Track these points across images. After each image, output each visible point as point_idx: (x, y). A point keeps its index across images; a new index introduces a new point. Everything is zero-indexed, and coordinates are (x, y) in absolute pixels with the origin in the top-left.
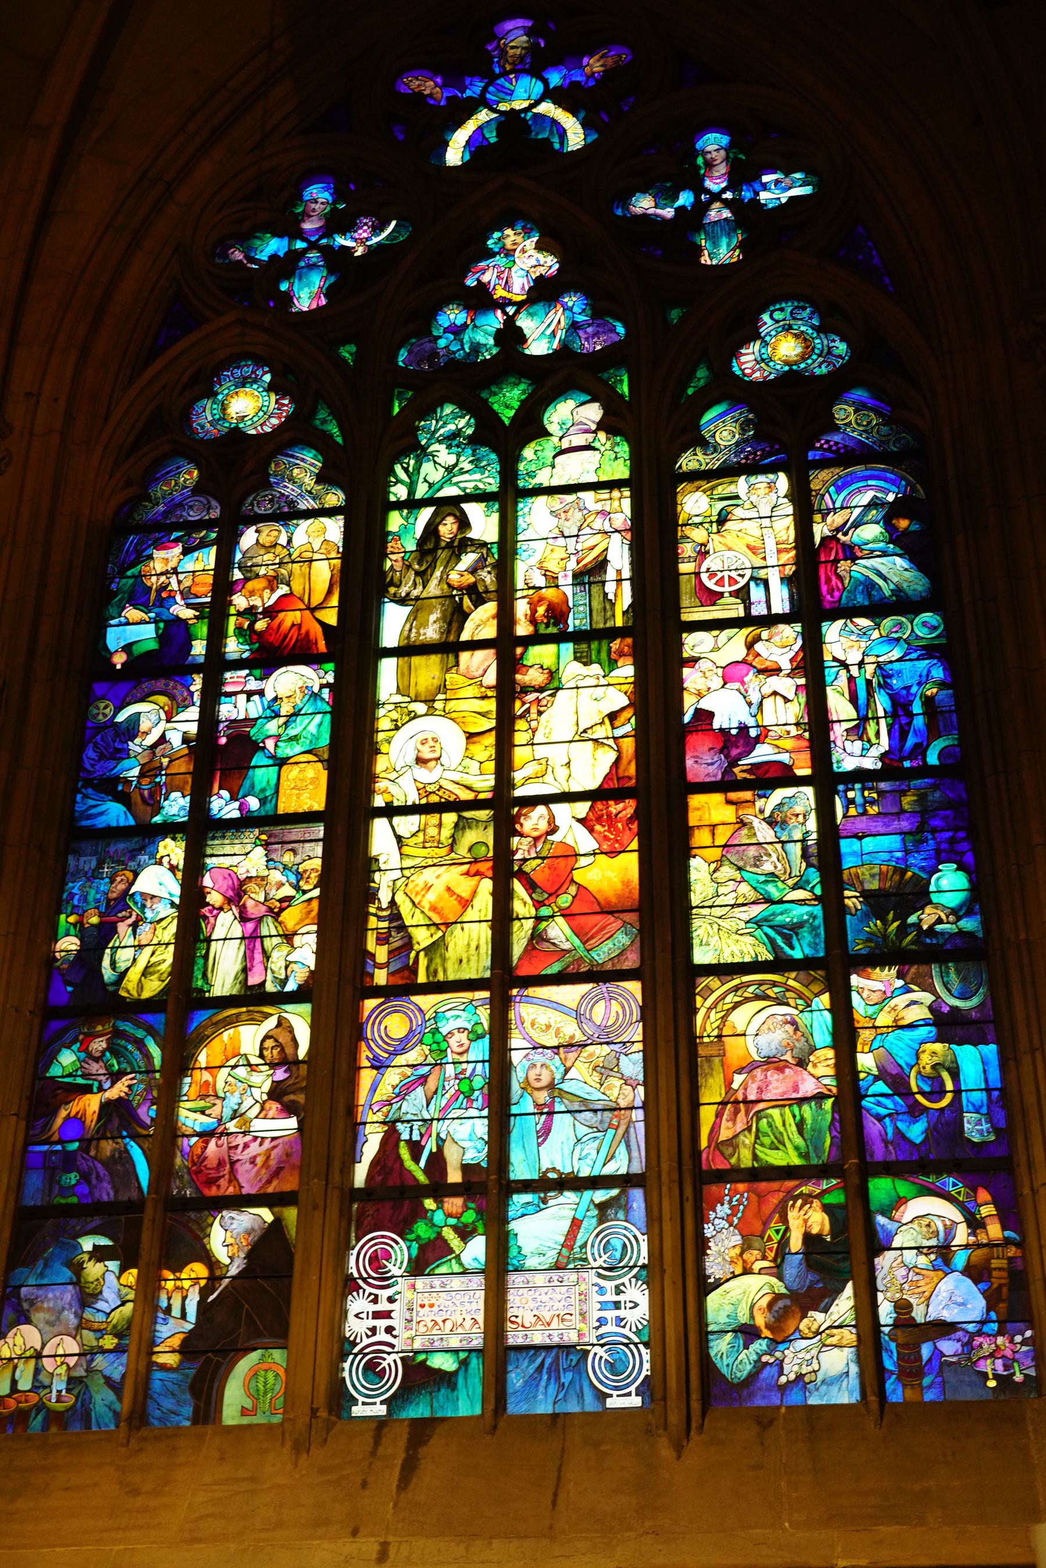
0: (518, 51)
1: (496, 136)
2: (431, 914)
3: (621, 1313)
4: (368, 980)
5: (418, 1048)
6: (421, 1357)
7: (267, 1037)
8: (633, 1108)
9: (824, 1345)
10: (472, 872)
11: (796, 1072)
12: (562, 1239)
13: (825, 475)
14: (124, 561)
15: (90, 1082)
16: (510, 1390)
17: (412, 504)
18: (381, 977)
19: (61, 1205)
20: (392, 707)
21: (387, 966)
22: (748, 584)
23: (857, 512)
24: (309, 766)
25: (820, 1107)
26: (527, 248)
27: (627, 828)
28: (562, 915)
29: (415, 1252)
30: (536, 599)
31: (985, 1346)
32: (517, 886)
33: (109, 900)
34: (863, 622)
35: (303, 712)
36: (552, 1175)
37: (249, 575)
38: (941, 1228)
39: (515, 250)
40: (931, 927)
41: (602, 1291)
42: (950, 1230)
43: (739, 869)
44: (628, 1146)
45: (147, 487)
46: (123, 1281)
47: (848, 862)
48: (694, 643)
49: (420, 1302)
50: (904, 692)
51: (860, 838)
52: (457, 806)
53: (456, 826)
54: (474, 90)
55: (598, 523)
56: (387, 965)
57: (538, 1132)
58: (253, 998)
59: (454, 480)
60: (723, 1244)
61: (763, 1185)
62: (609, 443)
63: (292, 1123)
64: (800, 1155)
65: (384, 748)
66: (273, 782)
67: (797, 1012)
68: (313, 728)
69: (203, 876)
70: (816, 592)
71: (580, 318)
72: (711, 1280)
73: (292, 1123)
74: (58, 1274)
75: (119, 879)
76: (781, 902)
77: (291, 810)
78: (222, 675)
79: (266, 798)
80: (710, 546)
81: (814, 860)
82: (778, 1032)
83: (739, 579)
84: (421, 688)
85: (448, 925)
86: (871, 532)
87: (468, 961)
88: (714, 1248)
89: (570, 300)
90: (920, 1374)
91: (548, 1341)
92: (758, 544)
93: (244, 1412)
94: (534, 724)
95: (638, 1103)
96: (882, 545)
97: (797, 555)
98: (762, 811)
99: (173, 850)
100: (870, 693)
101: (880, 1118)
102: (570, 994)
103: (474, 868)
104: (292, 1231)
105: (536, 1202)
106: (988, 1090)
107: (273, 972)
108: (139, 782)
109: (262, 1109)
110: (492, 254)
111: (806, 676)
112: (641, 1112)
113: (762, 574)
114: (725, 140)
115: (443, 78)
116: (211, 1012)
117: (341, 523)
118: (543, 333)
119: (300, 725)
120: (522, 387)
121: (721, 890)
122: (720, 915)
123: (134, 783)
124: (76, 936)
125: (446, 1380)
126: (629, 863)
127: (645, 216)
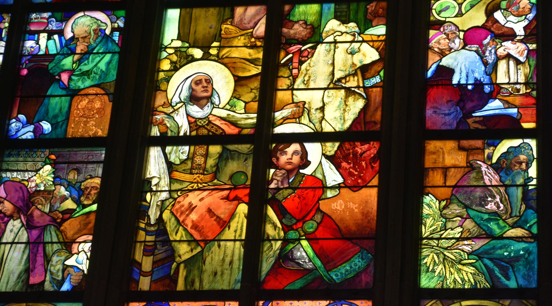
2: (193, 232)
4: (134, 285)
10: (232, 196)
18: (145, 284)
20: (171, 51)
21: (151, 275)
27: (370, 167)
32: (271, 213)
35: (95, 51)
43: (466, 207)
52: (222, 139)
56: (151, 273)
65: (163, 88)
66: (65, 110)
68: (102, 66)
76: (501, 238)
77: (78, 135)
78: (28, 15)
79: (58, 123)
81: (533, 203)
84: (199, 35)
85: (207, 242)
87: (222, 274)
94: (295, 71)
98: (490, 157)
103: (233, 194)
111: (536, 42)
119: (92, 62)
121: (449, 225)
122: (446, 246)
126: (370, 195)
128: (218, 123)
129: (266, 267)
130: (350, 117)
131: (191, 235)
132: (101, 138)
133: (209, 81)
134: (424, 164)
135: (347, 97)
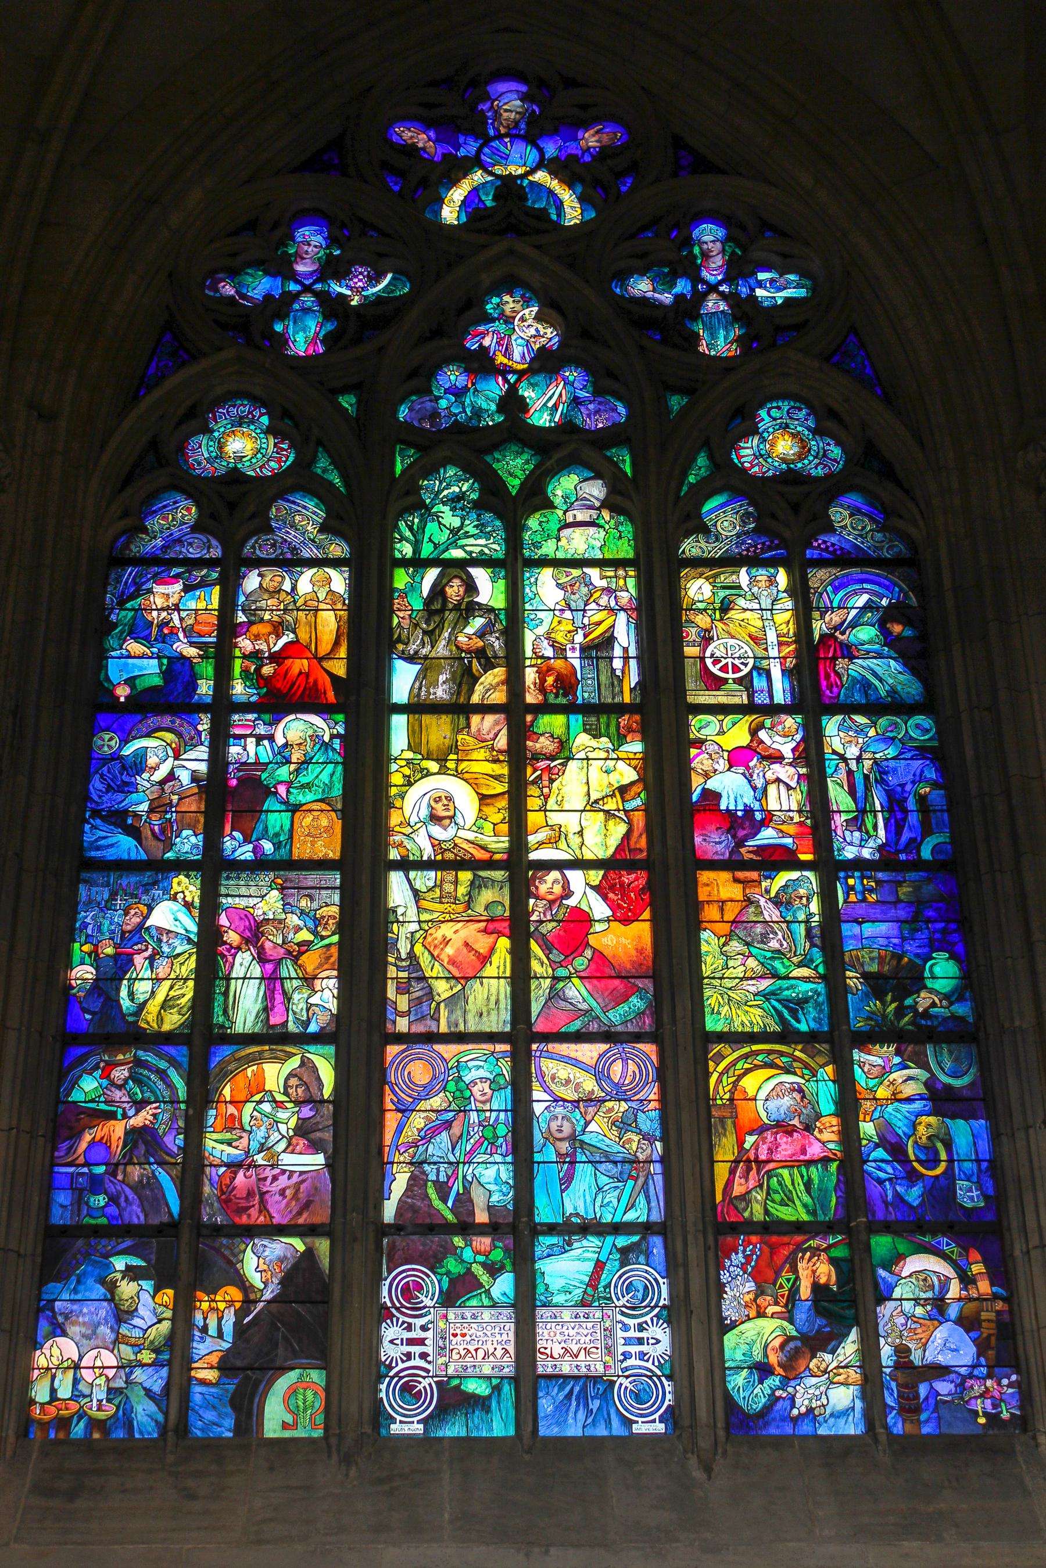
0: (513, 115)
1: (493, 200)
2: (450, 967)
3: (644, 1348)
5: (442, 1094)
6: (456, 1382)
9: (832, 1383)
11: (803, 1137)
12: (587, 1279)
14: (123, 592)
16: (541, 1414)
17: (418, 563)
19: (90, 1226)
22: (750, 673)
23: (853, 612)
25: (826, 1168)
28: (581, 978)
29: (445, 1286)
32: (534, 946)
33: (123, 933)
34: (861, 719)
38: (936, 1282)
40: (926, 1010)
41: (626, 1328)
43: (747, 944)
45: (144, 519)
46: (158, 1299)
47: (849, 946)
50: (899, 789)
51: (860, 923)
53: (472, 883)
54: (469, 148)
56: (408, 1013)
58: (274, 1038)
60: (738, 1288)
61: (774, 1238)
62: (613, 522)
63: (320, 1159)
64: (808, 1212)
65: (398, 804)
66: (287, 827)
68: (325, 777)
70: (816, 684)
71: (582, 394)
73: (320, 1159)
74: (91, 1290)
75: (133, 912)
76: (787, 978)
77: (306, 856)
80: (714, 633)
83: (742, 667)
84: (433, 746)
86: (866, 634)
88: (729, 1293)
89: (571, 374)
90: (917, 1410)
92: (760, 634)
93: (285, 1426)
96: (877, 647)
98: (768, 891)
99: (187, 886)
100: (867, 788)
101: (880, 1182)
102: (589, 1052)
104: (325, 1262)
106: (978, 1161)
107: (294, 1013)
109: (289, 1144)
110: (490, 319)
111: (807, 766)
112: (658, 1166)
114: (721, 233)
116: (235, 1047)
117: (346, 575)
118: (545, 405)
120: (525, 456)
121: (731, 963)
125: (480, 1403)
126: (641, 930)
128: (465, 846)
129: (535, 1008)
130: (614, 842)
132: (332, 861)
133: (450, 799)
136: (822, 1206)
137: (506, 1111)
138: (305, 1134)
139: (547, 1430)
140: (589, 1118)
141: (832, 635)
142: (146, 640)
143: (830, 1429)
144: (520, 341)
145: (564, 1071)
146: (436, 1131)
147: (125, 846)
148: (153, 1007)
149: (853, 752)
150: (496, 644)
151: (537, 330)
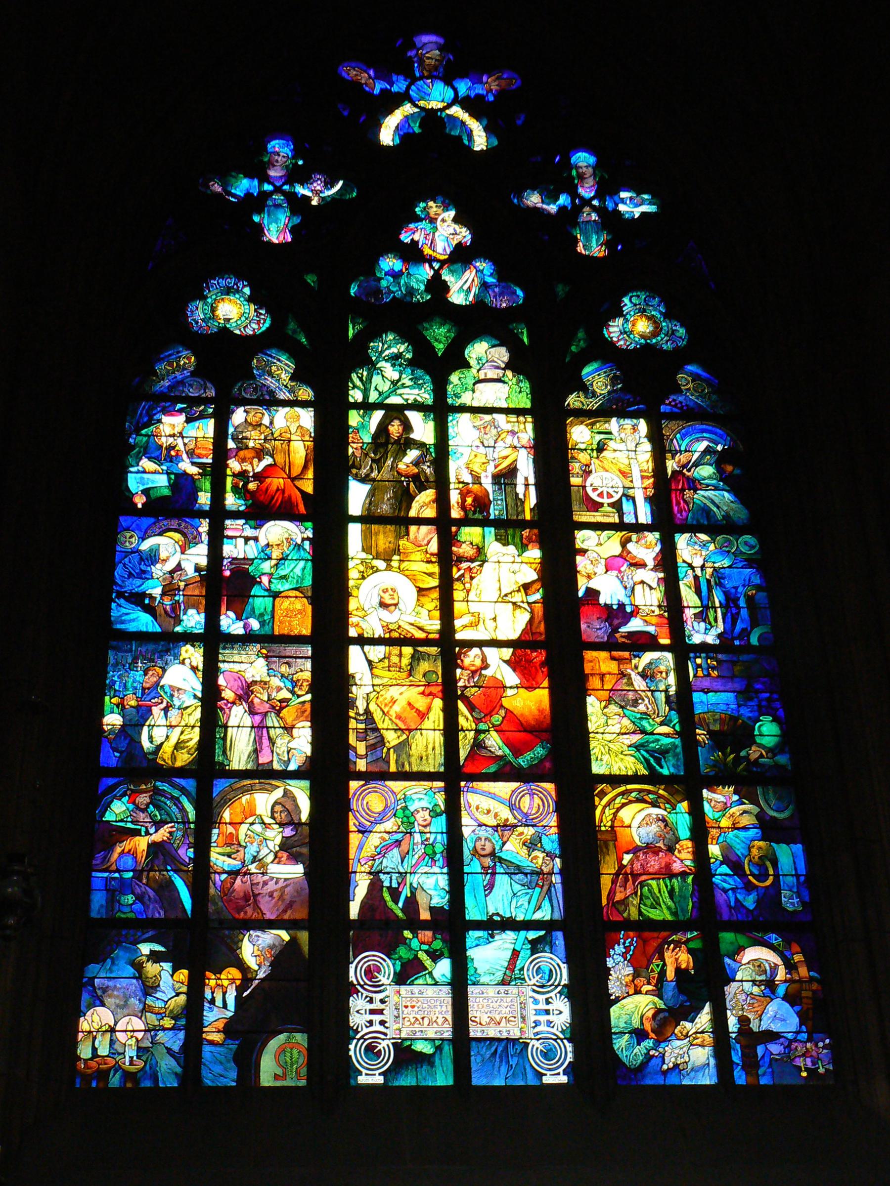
1: (420, 127)
5: (393, 819)
6: (409, 1043)
7: (276, 803)
8: (553, 873)
9: (692, 1045)
10: (427, 692)
12: (506, 964)
13: (673, 425)
14: (138, 422)
15: (139, 827)
17: (366, 407)
18: (361, 765)
19: (121, 919)
20: (359, 561)
22: (621, 498)
23: (696, 455)
24: (297, 600)
26: (447, 218)
29: (398, 968)
30: (465, 491)
31: (799, 1049)
32: (461, 705)
34: (703, 537)
35: (289, 558)
36: (496, 918)
37: (240, 445)
38: (768, 968)
39: (436, 219)
40: (756, 760)
41: (536, 1001)
42: (774, 968)
43: (622, 707)
44: (551, 900)
47: (698, 710)
48: (583, 538)
49: (404, 1004)
50: (733, 591)
51: (706, 693)
53: (413, 656)
55: (509, 439)
56: (366, 756)
57: (485, 887)
58: (263, 775)
59: (399, 391)
61: (647, 934)
62: (514, 380)
64: (672, 913)
65: (354, 592)
66: (269, 609)
67: (665, 813)
68: (298, 571)
69: (218, 677)
71: (490, 280)
72: (612, 997)
75: (151, 673)
76: (652, 733)
77: (286, 632)
79: (265, 621)
80: (592, 467)
82: (653, 826)
84: (381, 550)
85: (410, 730)
86: (706, 471)
87: (427, 756)
89: (481, 265)
91: (499, 1035)
92: (627, 470)
93: (277, 1078)
94: (468, 586)
95: (556, 870)
96: (714, 482)
97: (654, 483)
98: (636, 667)
99: (194, 655)
101: (725, 891)
102: (504, 788)
105: (486, 936)
106: (797, 876)
107: (278, 754)
108: (161, 598)
109: (276, 857)
110: (418, 219)
113: (631, 492)
114: (592, 160)
115: (375, 72)
116: (233, 781)
117: (312, 414)
118: (461, 287)
120: (447, 327)
121: (610, 722)
123: (158, 599)
124: (119, 714)
127: (535, 210)
129: (463, 754)
131: (397, 725)
132: (304, 636)
134: (584, 671)
135: (514, 610)
136: (682, 910)
137: (442, 833)
138: (288, 850)
139: (478, 1079)
140: (505, 839)
141: (681, 472)
142: (157, 460)
143: (691, 1081)
144: (442, 238)
145: (486, 803)
146: (387, 848)
147: (143, 622)
148: (168, 748)
149: (698, 562)
150: (428, 471)
151: (455, 230)
